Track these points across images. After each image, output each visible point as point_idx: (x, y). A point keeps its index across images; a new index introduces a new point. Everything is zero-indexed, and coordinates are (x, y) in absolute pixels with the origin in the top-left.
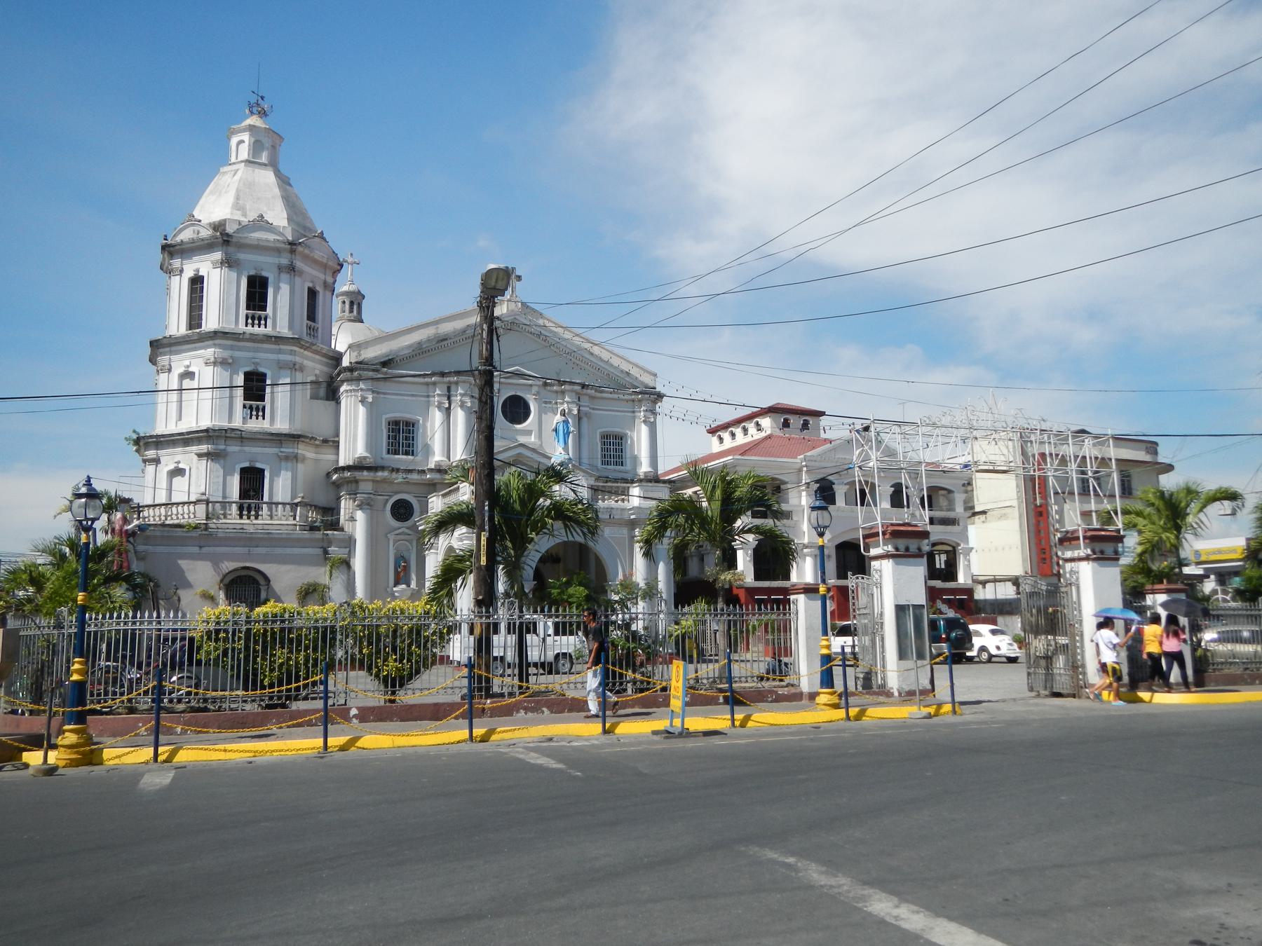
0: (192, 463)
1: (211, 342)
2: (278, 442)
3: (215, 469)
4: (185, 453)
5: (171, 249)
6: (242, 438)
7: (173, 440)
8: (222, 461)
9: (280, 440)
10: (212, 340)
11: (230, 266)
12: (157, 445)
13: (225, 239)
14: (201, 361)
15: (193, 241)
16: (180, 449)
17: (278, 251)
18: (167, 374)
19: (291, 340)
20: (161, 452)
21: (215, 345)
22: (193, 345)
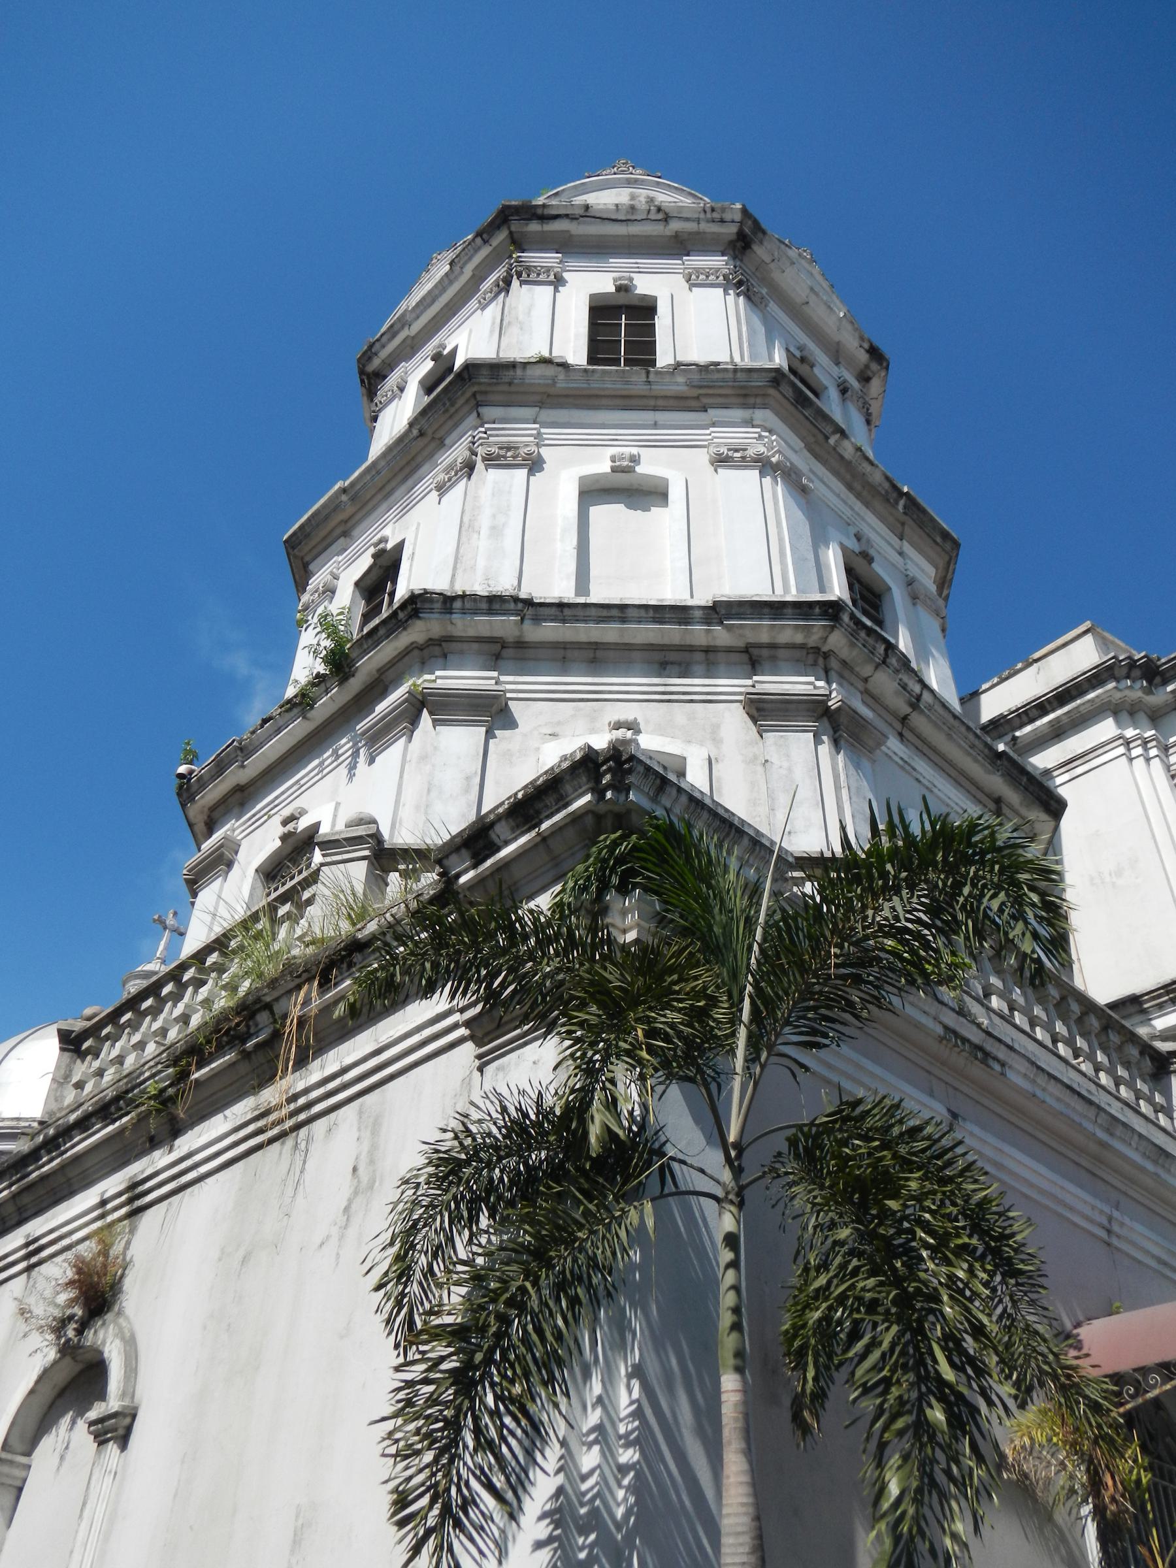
0: (717, 741)
1: (738, 414)
2: (992, 806)
3: (854, 785)
4: (667, 698)
5: (534, 227)
6: (904, 719)
7: (596, 646)
8: (866, 763)
9: (998, 801)
10: (745, 406)
11: (749, 298)
12: (498, 657)
13: (747, 230)
14: (702, 457)
15: (629, 215)
16: (639, 682)
17: (837, 354)
18: (525, 471)
19: (939, 540)
20: (512, 683)
21: (750, 423)
22: (649, 416)
